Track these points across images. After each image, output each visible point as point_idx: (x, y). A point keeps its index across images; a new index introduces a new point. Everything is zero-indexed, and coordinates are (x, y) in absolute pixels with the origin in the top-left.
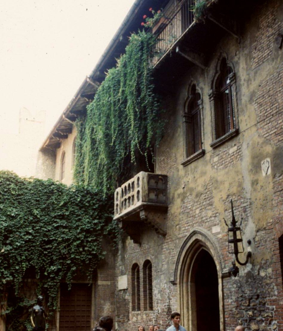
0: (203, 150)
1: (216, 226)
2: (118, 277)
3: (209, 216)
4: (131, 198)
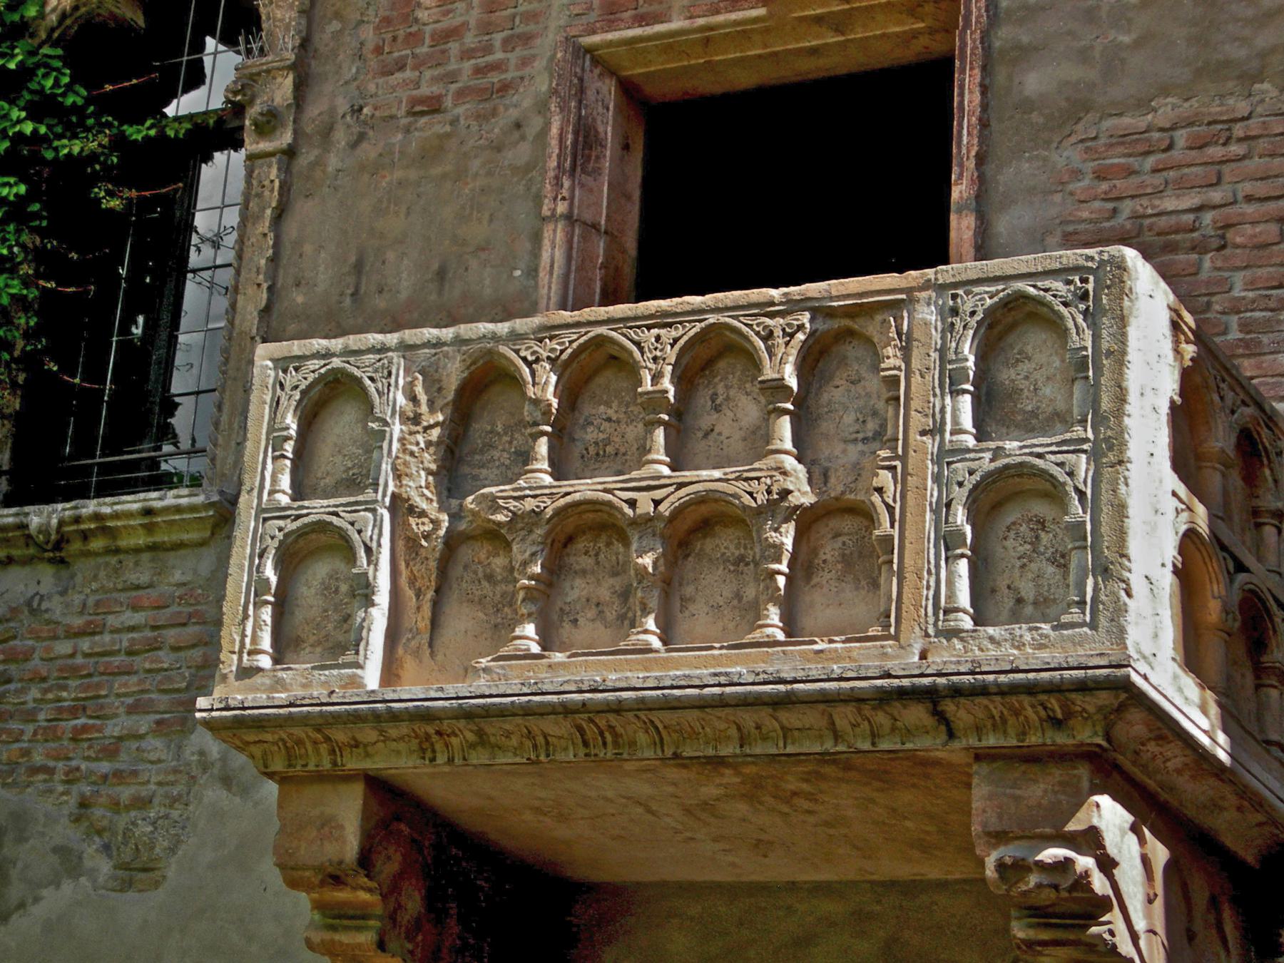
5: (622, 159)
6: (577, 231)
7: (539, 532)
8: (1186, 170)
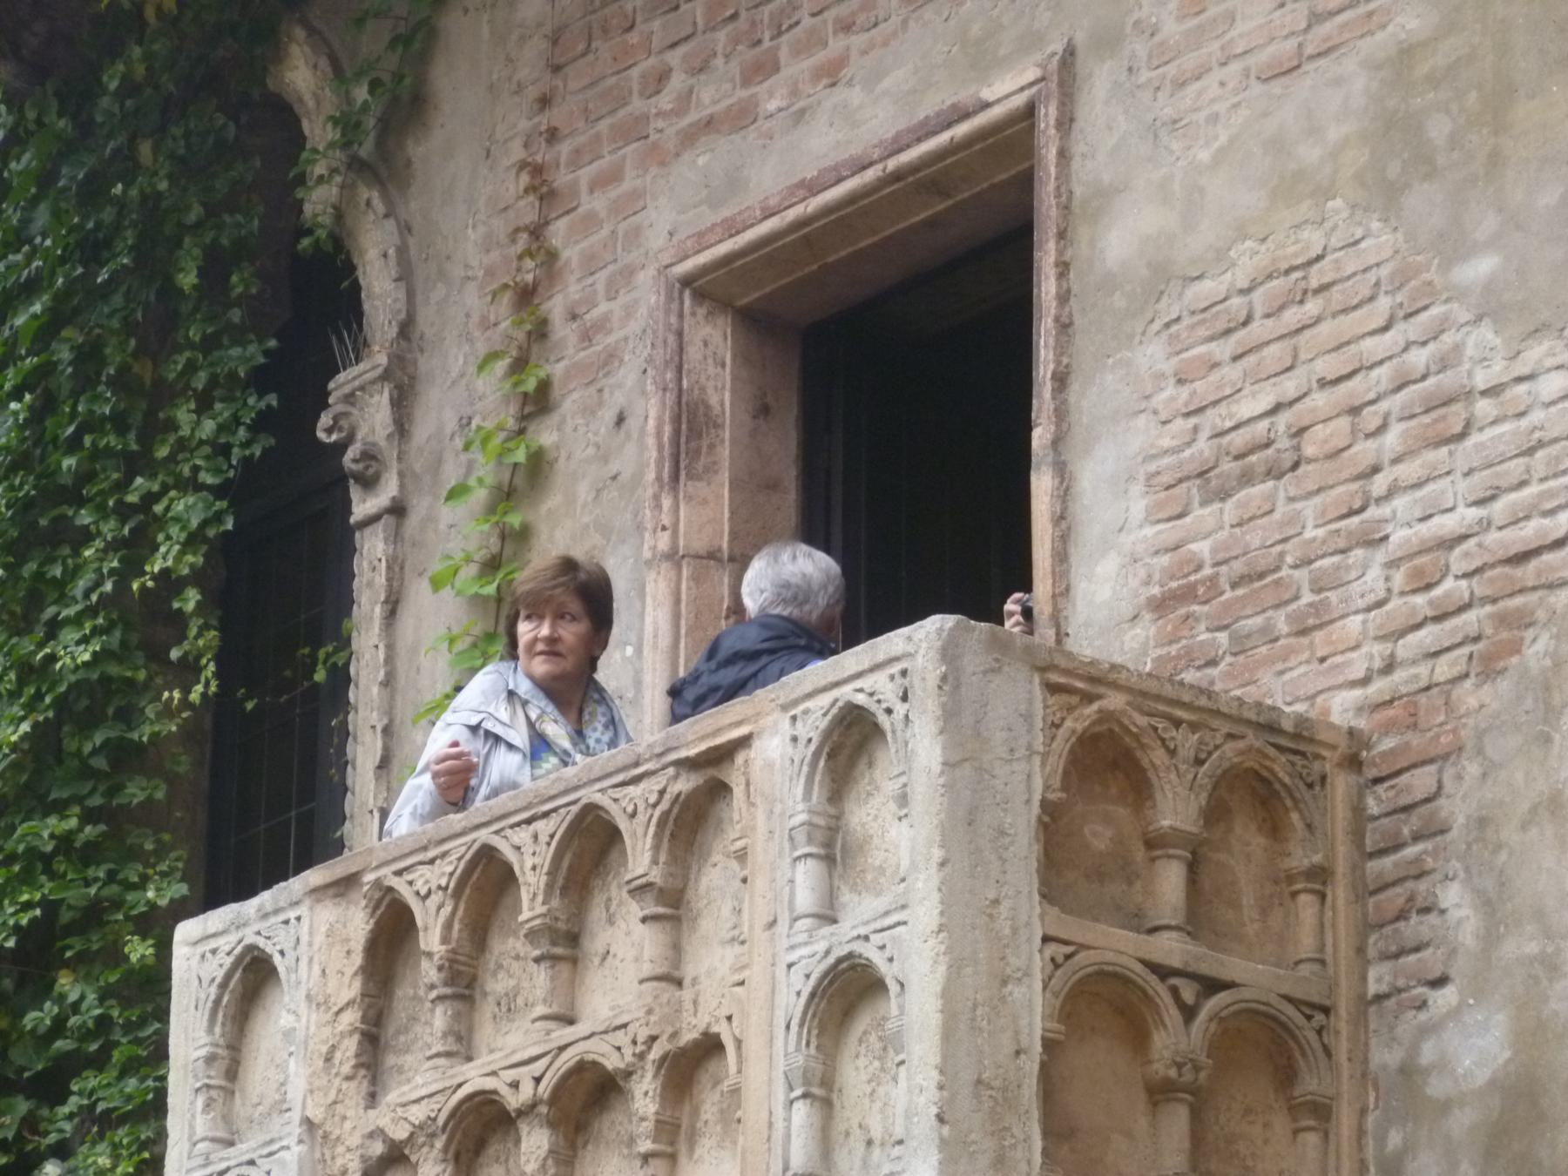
4: (645, 1097)
5: (754, 433)
6: (685, 573)
7: (439, 1144)
8: (1266, 351)
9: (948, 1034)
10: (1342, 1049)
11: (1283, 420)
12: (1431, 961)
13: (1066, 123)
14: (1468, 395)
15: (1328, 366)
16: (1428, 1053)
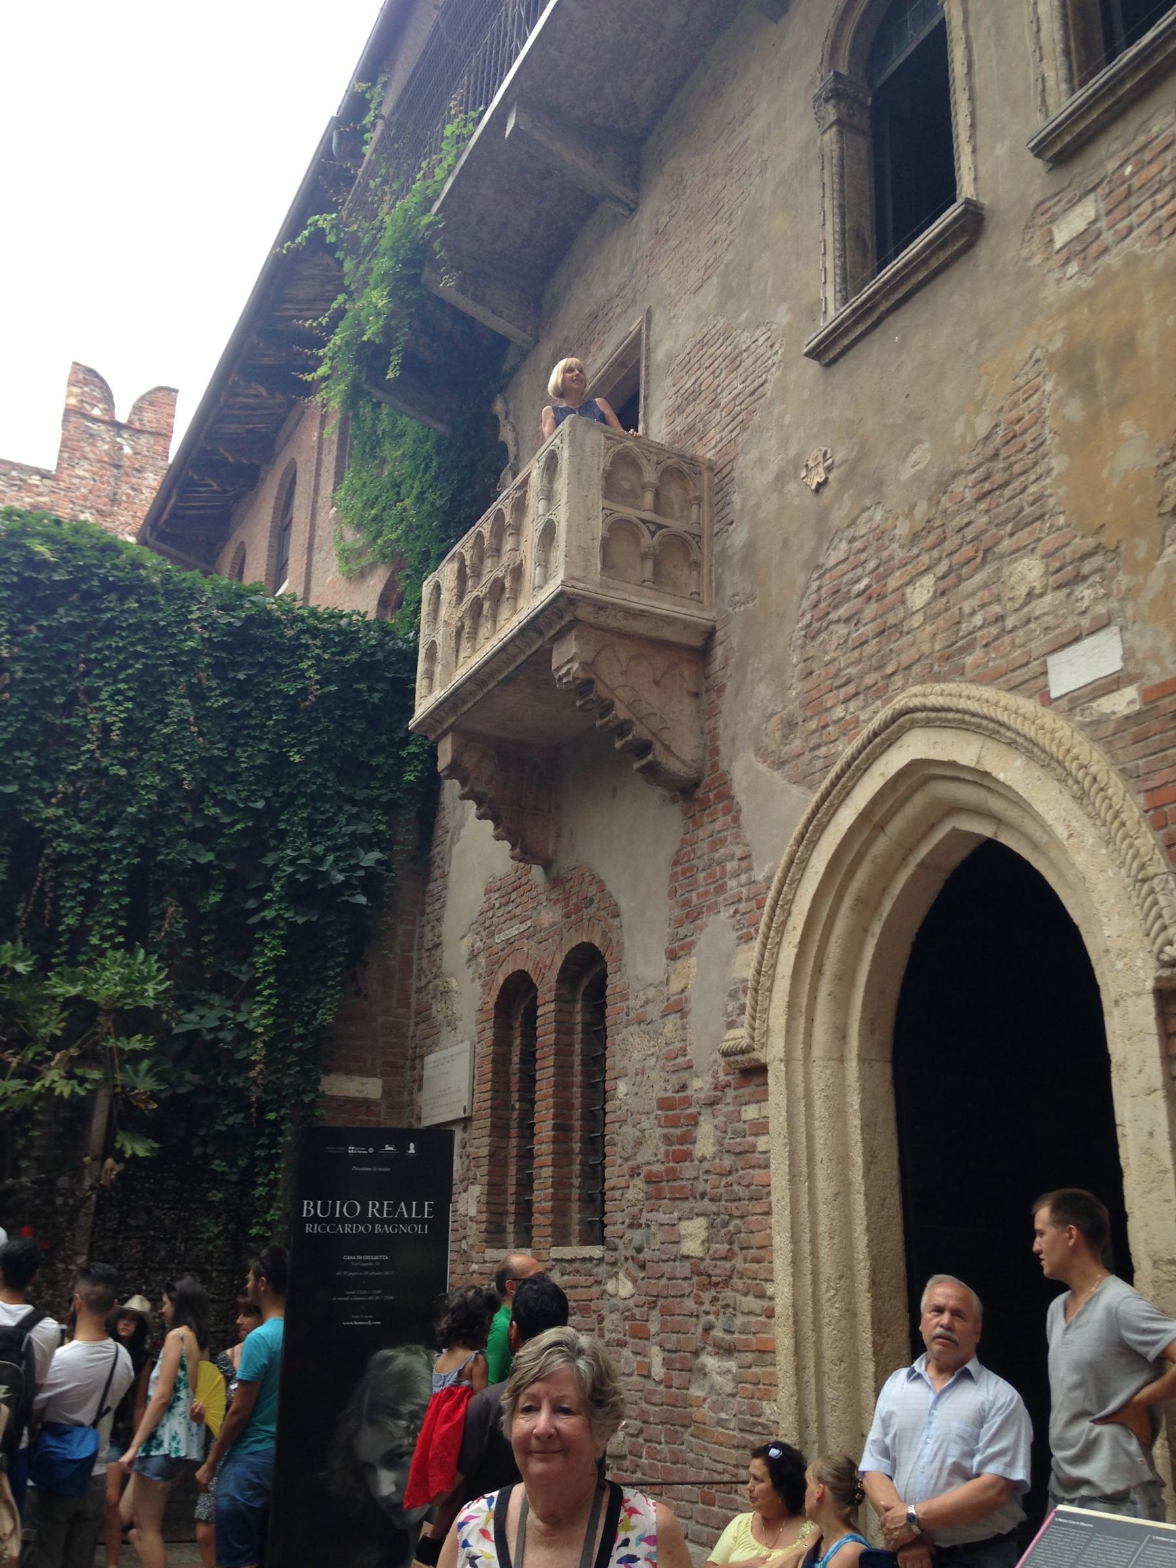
0: (968, 201)
1: (1087, 642)
2: (422, 1058)
3: (1023, 591)
9: (569, 532)
10: (705, 550)
11: (697, 385)
12: (730, 518)
13: (648, 329)
14: (741, 353)
15: (707, 364)
16: (728, 543)
